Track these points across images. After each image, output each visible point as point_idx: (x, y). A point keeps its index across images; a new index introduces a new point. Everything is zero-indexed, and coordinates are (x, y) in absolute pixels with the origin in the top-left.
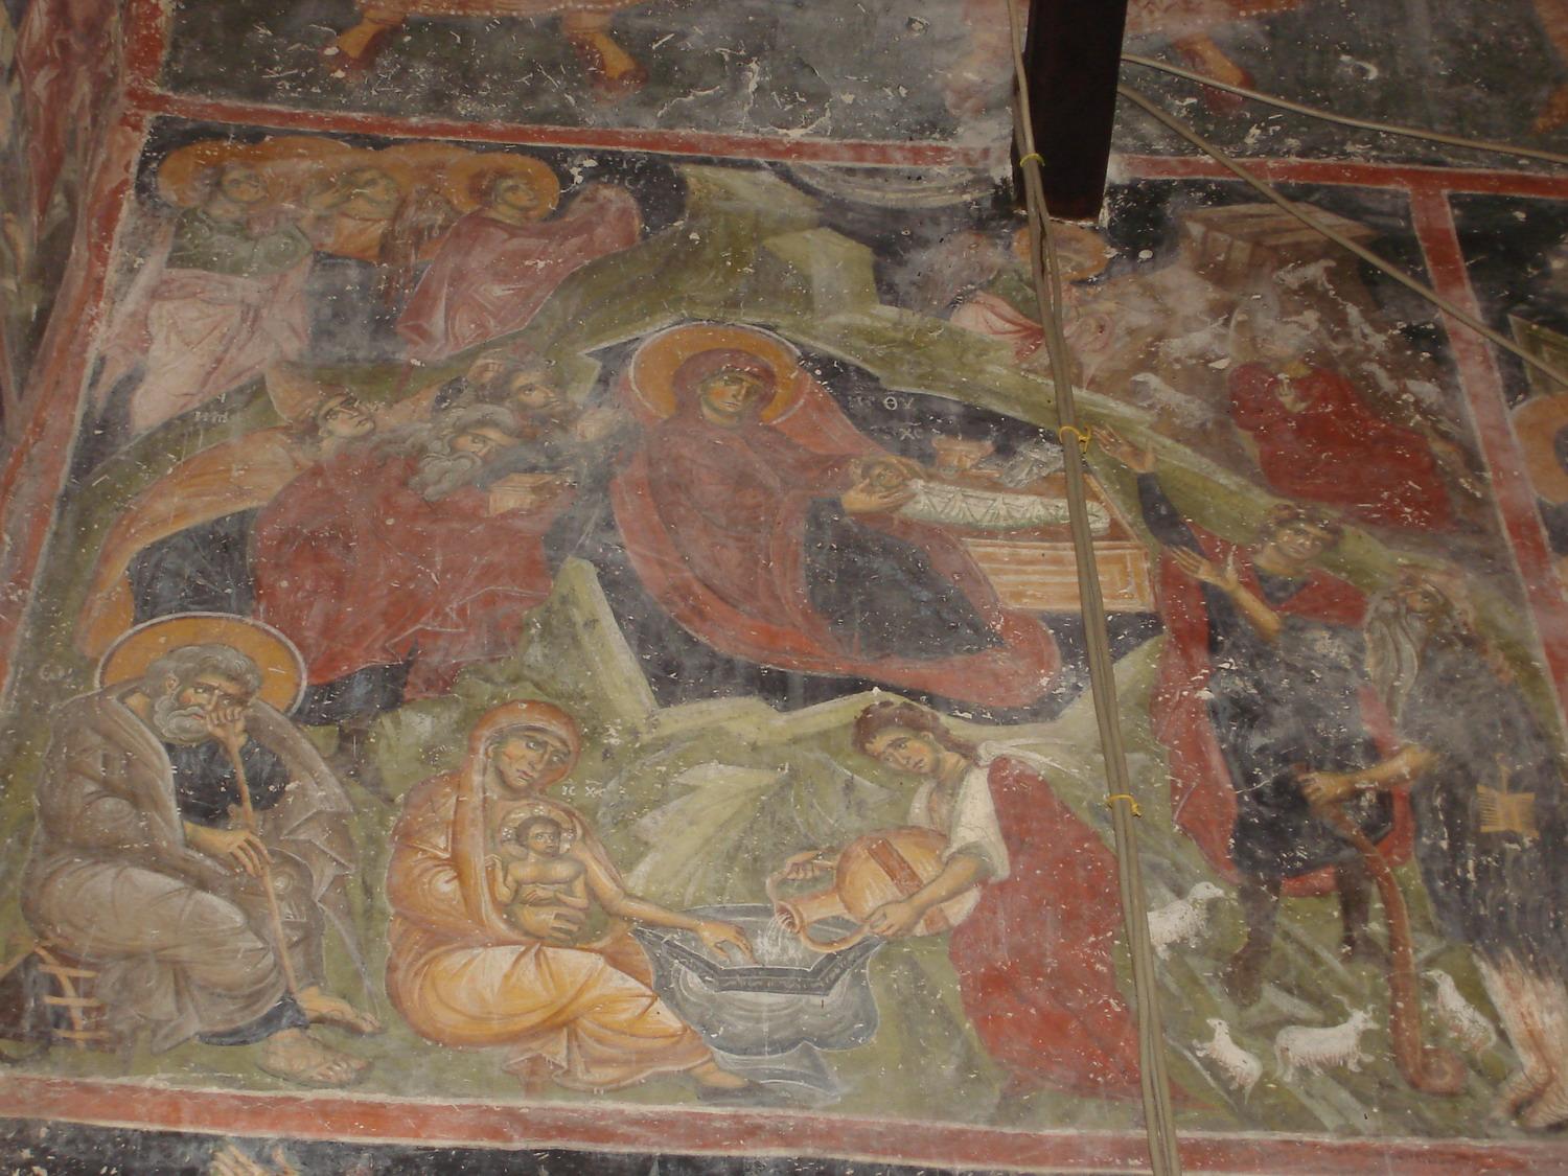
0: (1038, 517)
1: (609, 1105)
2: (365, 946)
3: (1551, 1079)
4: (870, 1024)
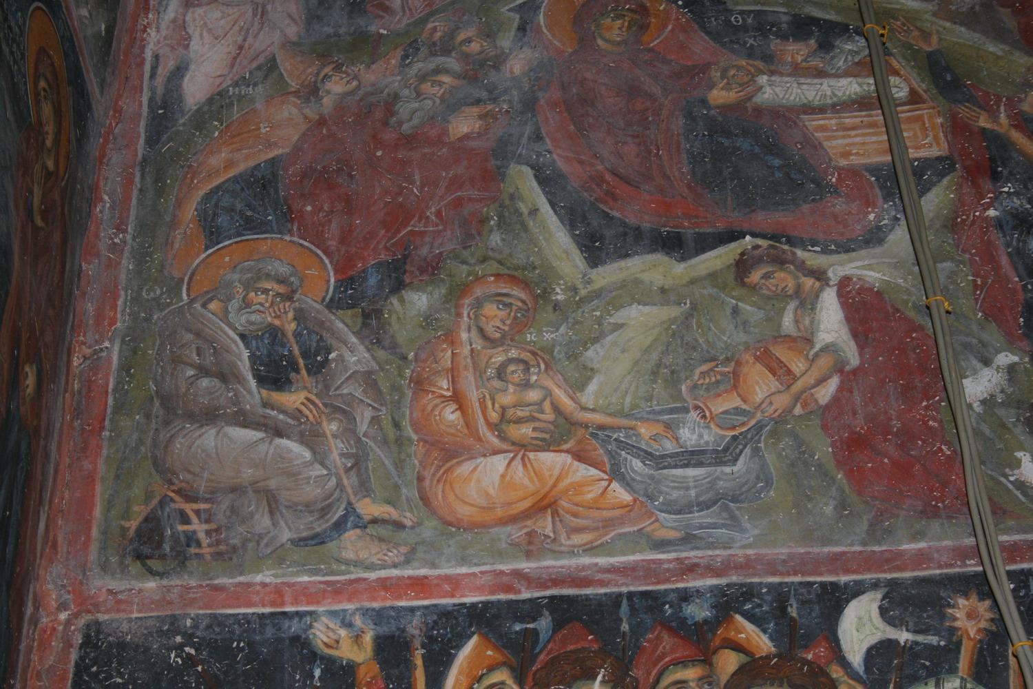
0: (856, 94)
1: (586, 560)
2: (399, 465)
4: (768, 483)
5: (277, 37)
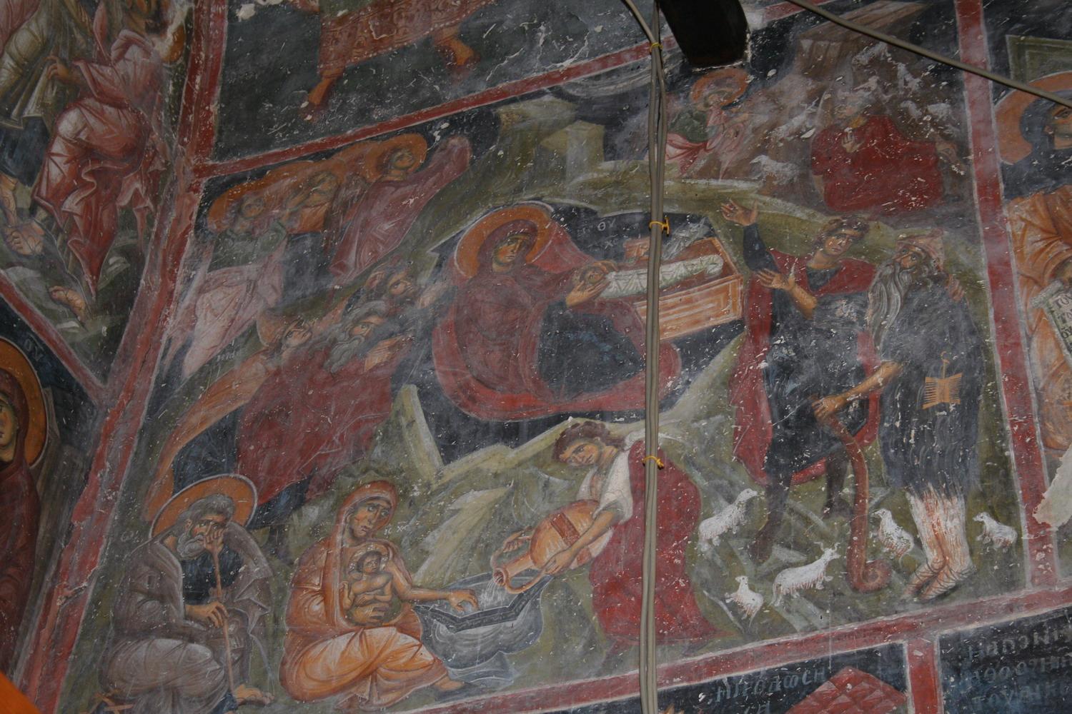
0: (681, 276)
2: (270, 656)
3: (945, 563)
4: (537, 631)
5: (260, 307)
